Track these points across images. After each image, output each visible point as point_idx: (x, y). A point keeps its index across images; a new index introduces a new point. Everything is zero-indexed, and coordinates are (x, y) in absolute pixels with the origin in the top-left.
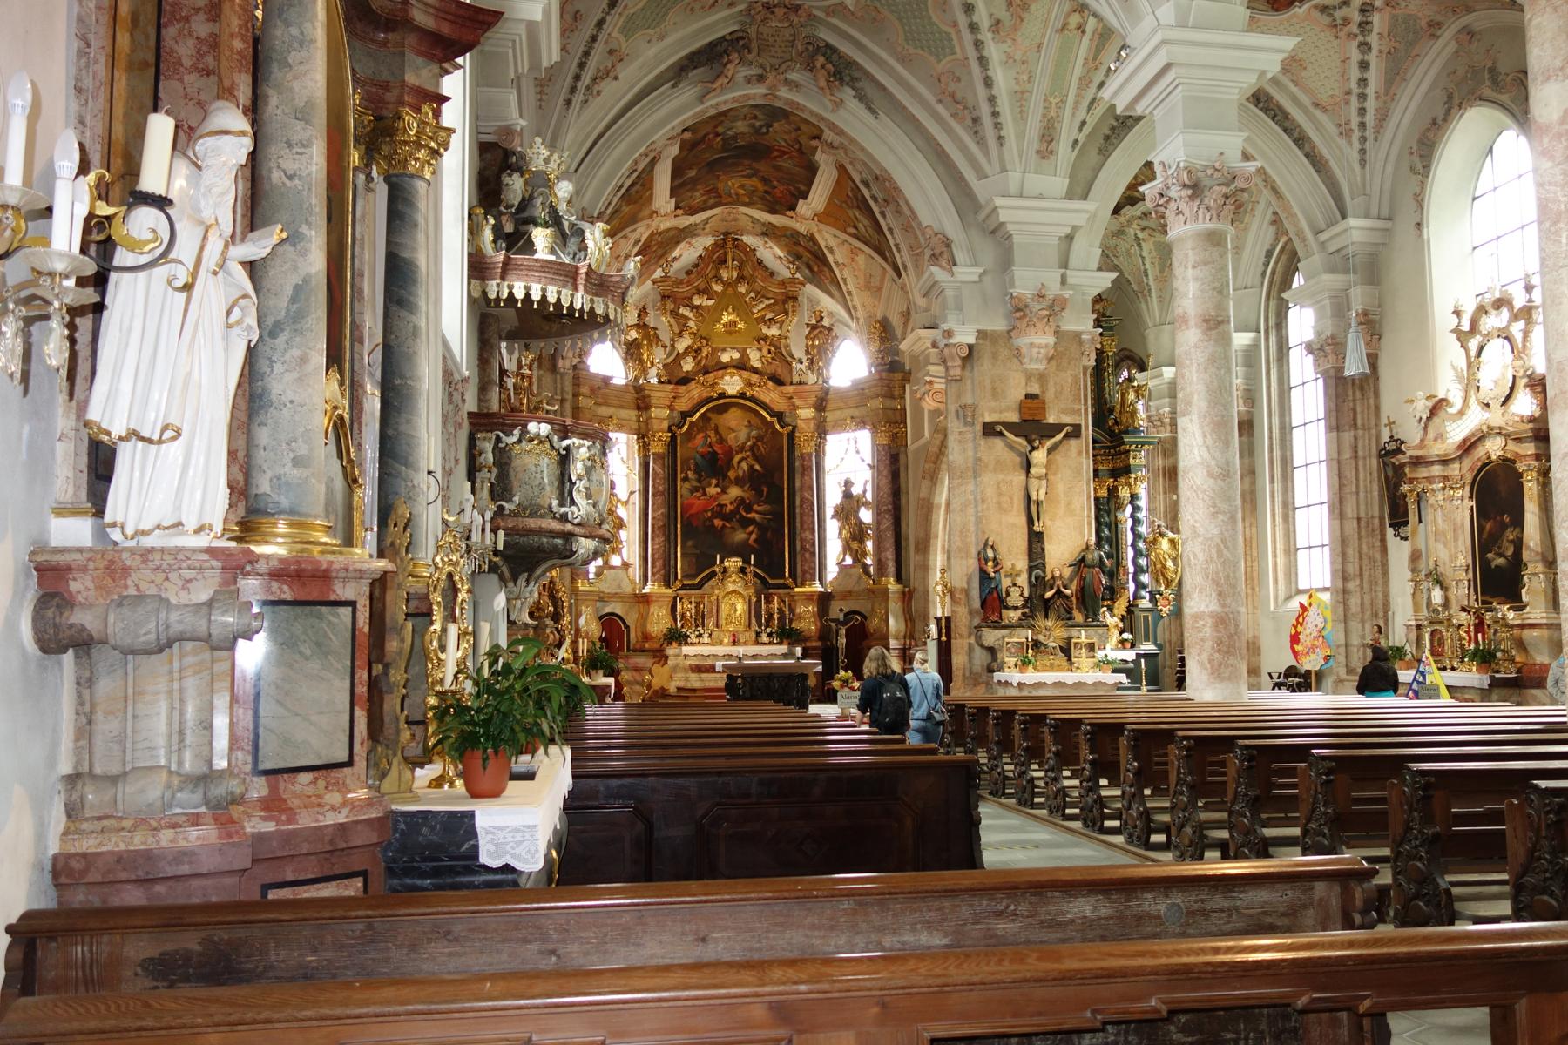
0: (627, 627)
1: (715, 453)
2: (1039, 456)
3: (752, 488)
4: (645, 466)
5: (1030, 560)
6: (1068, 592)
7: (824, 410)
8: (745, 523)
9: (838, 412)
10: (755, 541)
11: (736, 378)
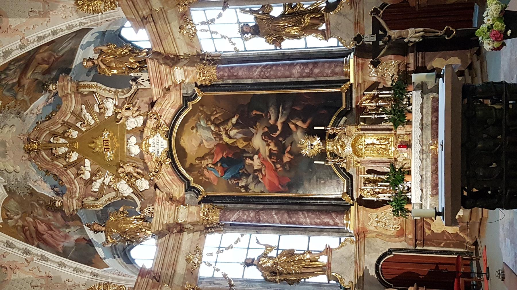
0: (390, 251)
1: (222, 160)
3: (253, 125)
4: (234, 227)
7: (178, 56)
8: (287, 132)
9: (178, 40)
10: (304, 122)
11: (150, 141)
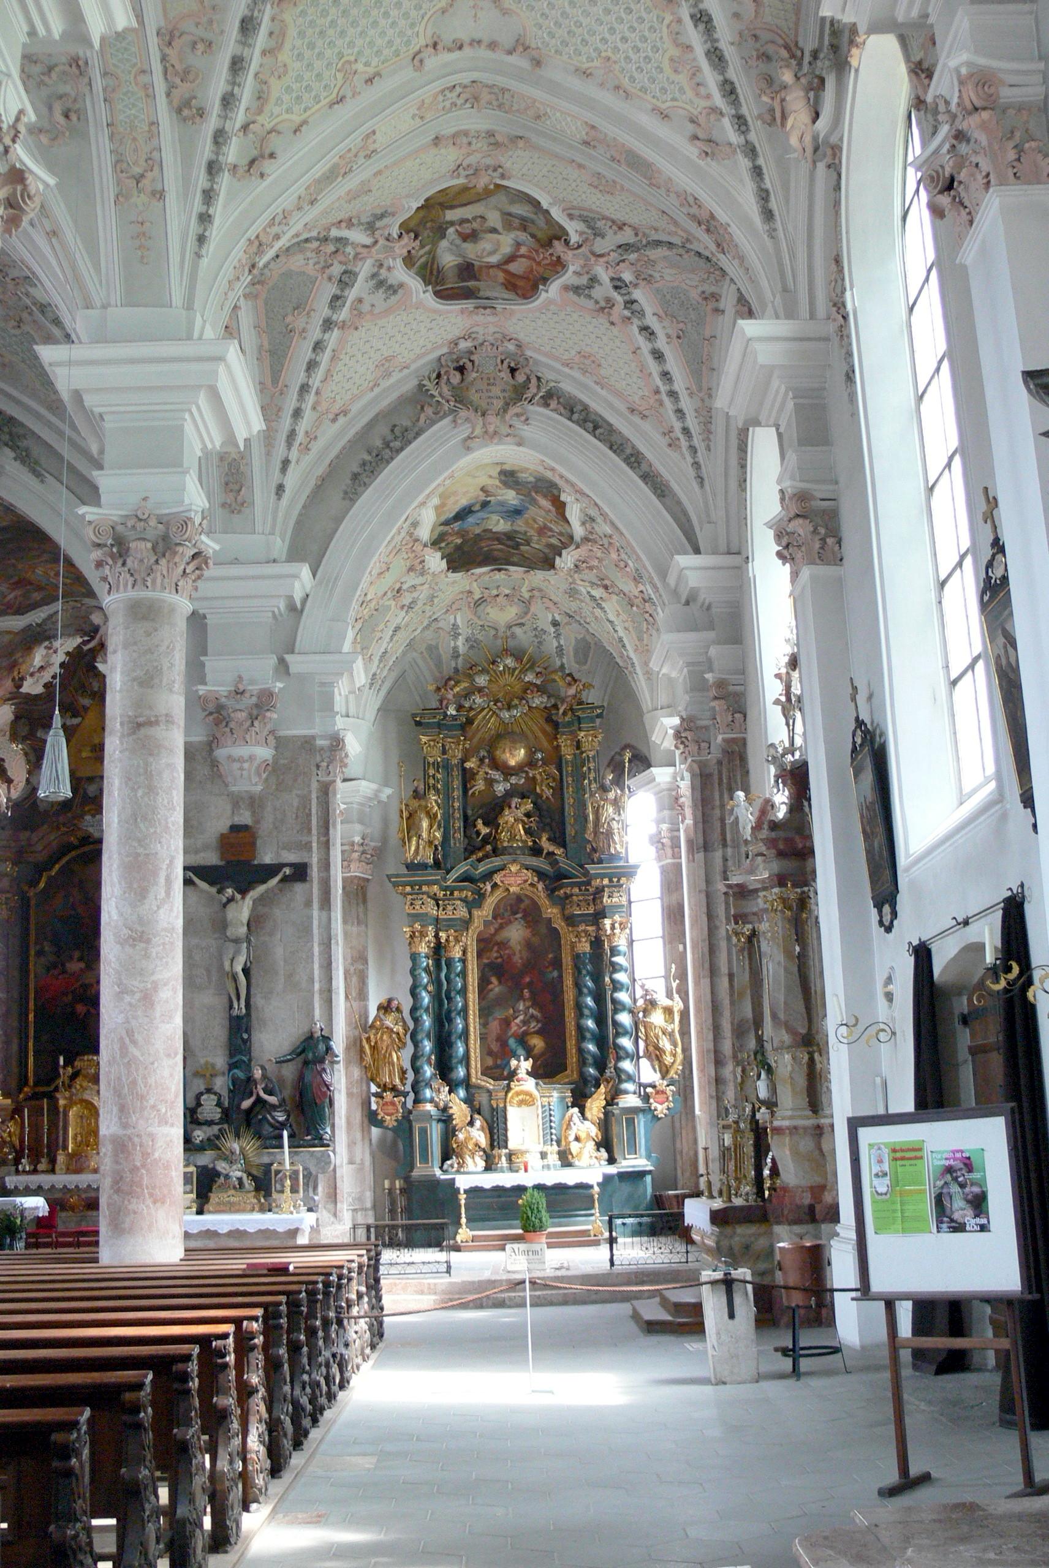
2: (242, 911)
5: (231, 1055)
6: (272, 1100)
